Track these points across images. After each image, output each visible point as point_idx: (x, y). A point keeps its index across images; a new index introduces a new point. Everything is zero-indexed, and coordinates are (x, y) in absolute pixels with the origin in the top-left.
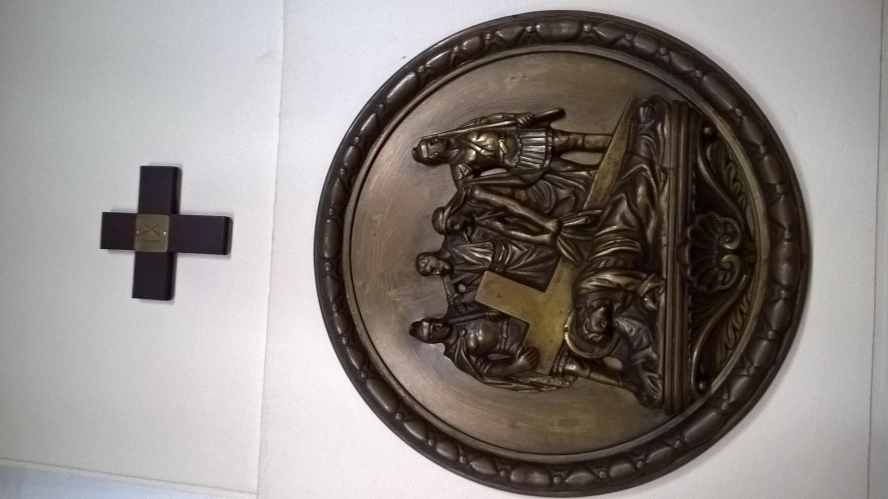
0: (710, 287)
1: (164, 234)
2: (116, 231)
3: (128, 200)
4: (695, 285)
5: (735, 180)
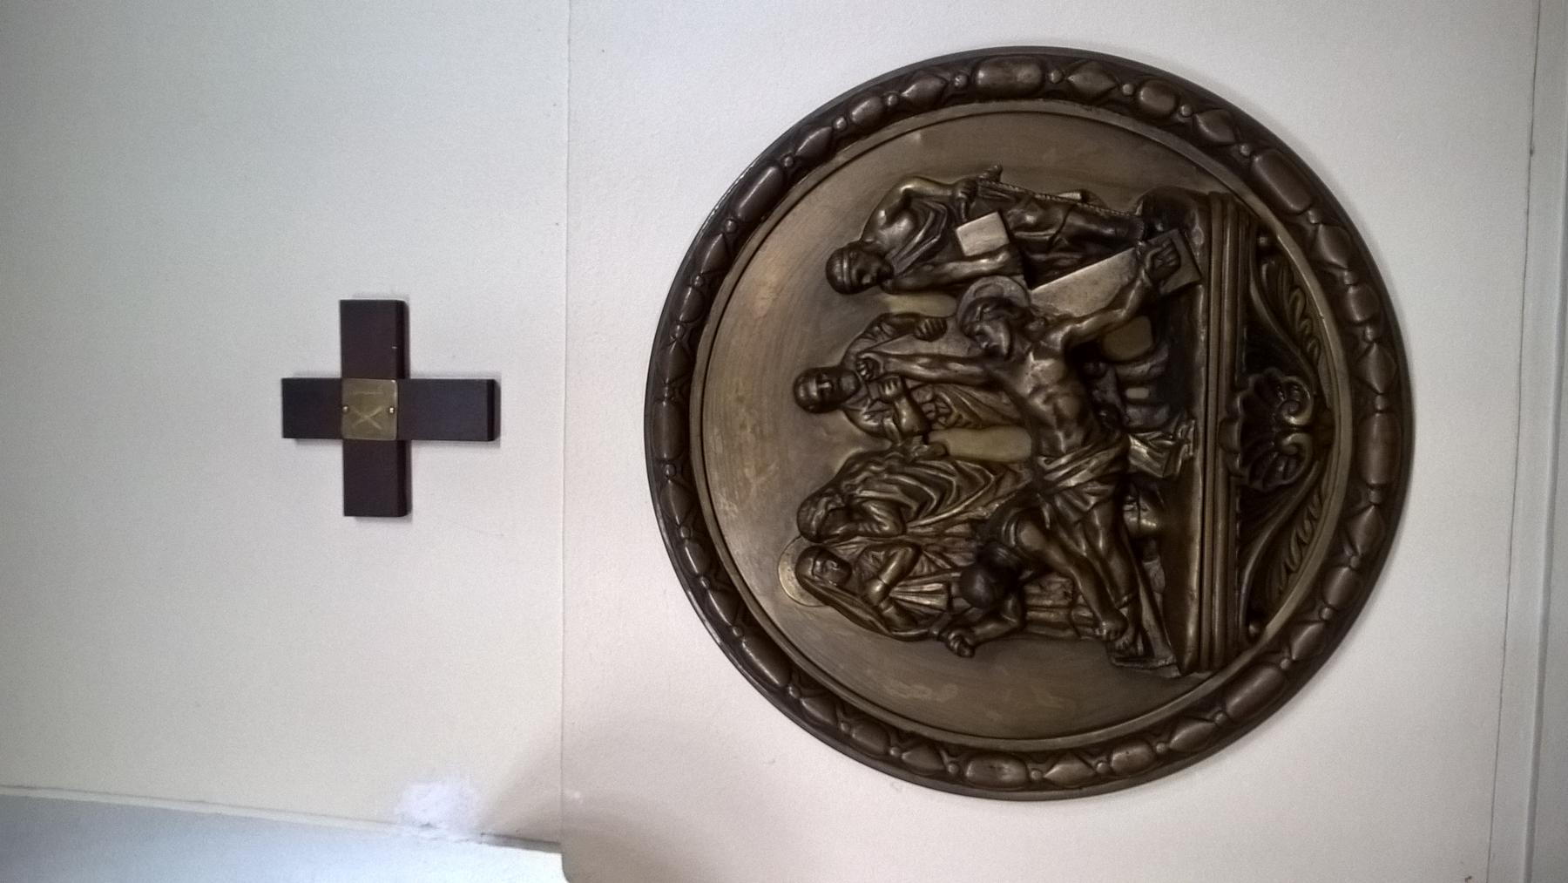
0: (1266, 481)
1: (382, 411)
2: (308, 409)
3: (326, 362)
4: (1246, 481)
5: (1304, 316)
